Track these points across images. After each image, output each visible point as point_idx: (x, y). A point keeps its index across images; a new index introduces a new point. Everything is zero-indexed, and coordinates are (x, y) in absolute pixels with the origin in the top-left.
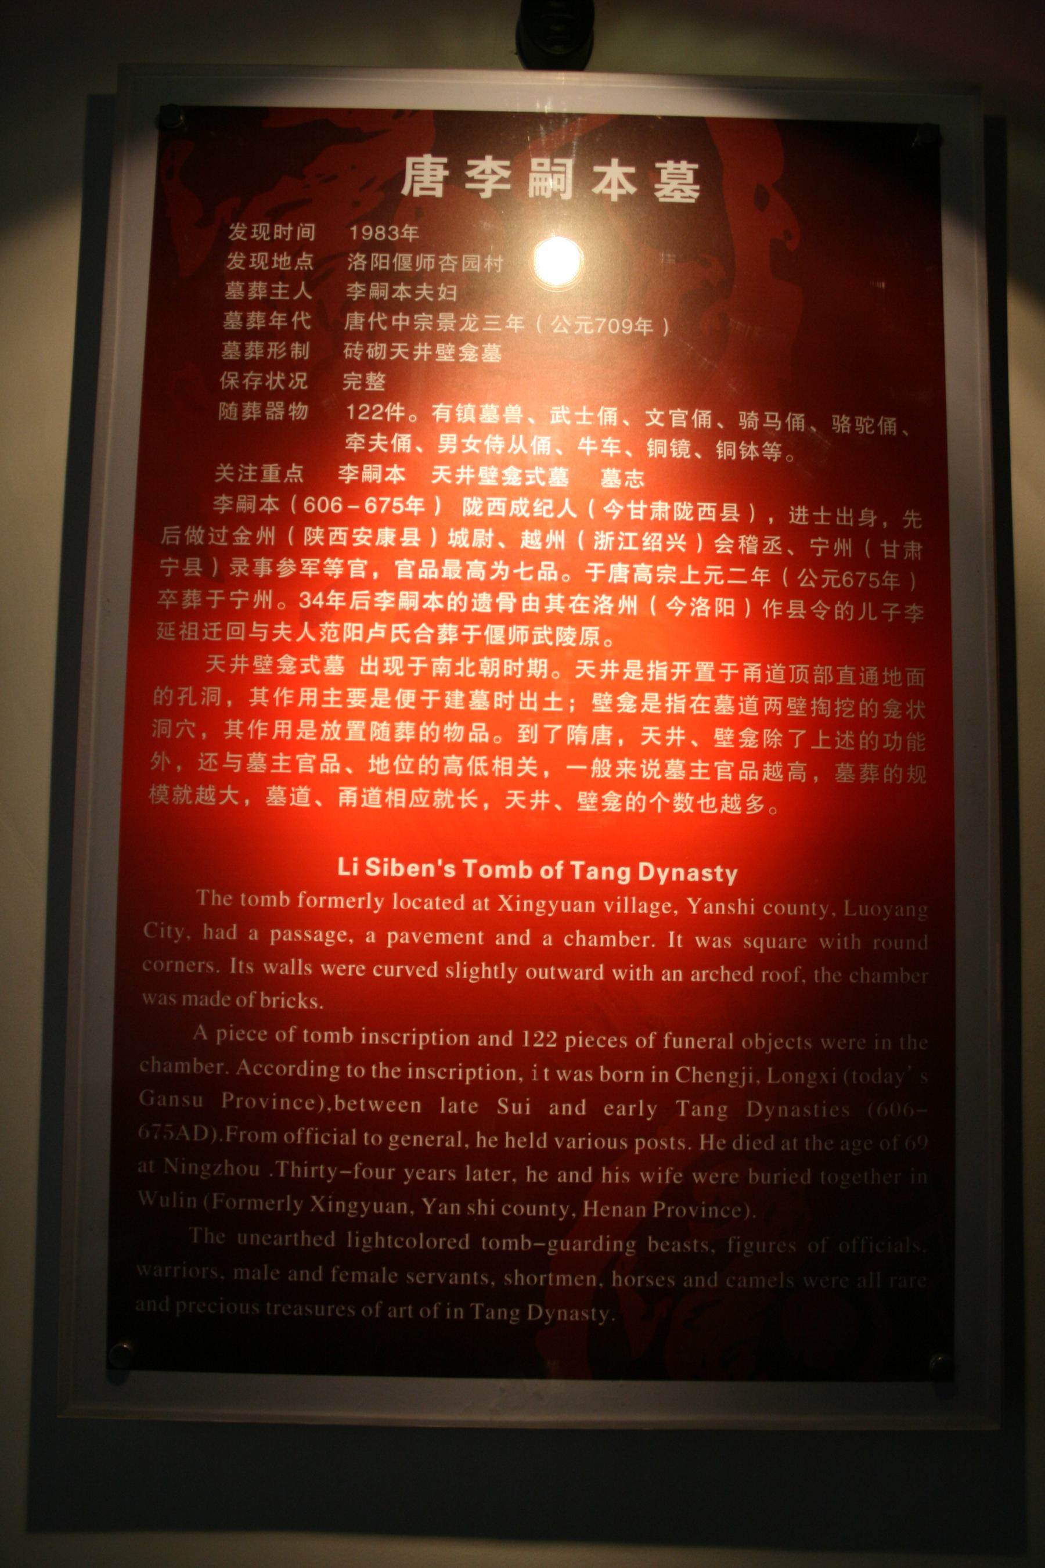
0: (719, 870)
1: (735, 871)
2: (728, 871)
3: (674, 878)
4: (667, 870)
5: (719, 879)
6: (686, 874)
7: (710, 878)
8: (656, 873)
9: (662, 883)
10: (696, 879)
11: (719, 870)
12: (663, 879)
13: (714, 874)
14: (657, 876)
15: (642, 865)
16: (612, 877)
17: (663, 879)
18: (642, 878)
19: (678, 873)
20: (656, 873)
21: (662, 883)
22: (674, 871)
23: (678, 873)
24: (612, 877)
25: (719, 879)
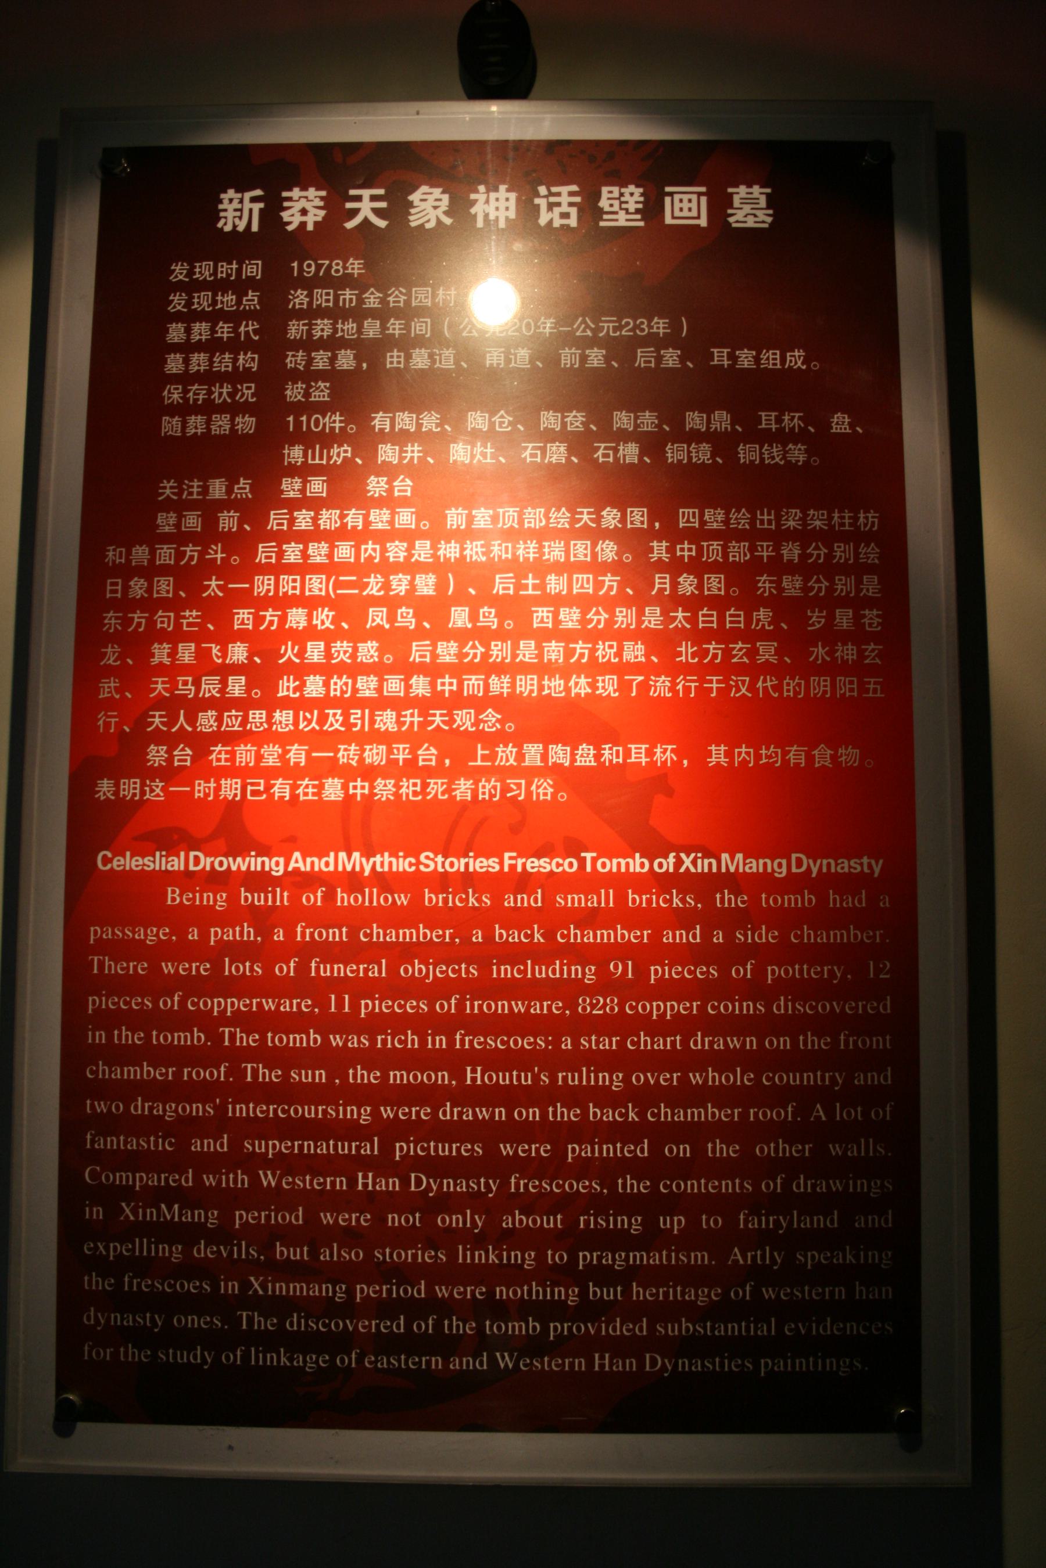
0: (865, 860)
1: (881, 862)
2: (873, 862)
3: (824, 870)
4: (819, 862)
5: (866, 870)
6: (837, 865)
7: (859, 869)
8: (809, 865)
9: (814, 875)
10: (846, 870)
11: (865, 860)
12: (815, 871)
13: (861, 864)
14: (809, 869)
15: (794, 856)
16: (769, 870)
17: (815, 871)
18: (794, 870)
19: (829, 865)
20: (809, 865)
21: (814, 875)
22: (825, 862)
23: (829, 865)
24: (769, 870)
25: (866, 870)
